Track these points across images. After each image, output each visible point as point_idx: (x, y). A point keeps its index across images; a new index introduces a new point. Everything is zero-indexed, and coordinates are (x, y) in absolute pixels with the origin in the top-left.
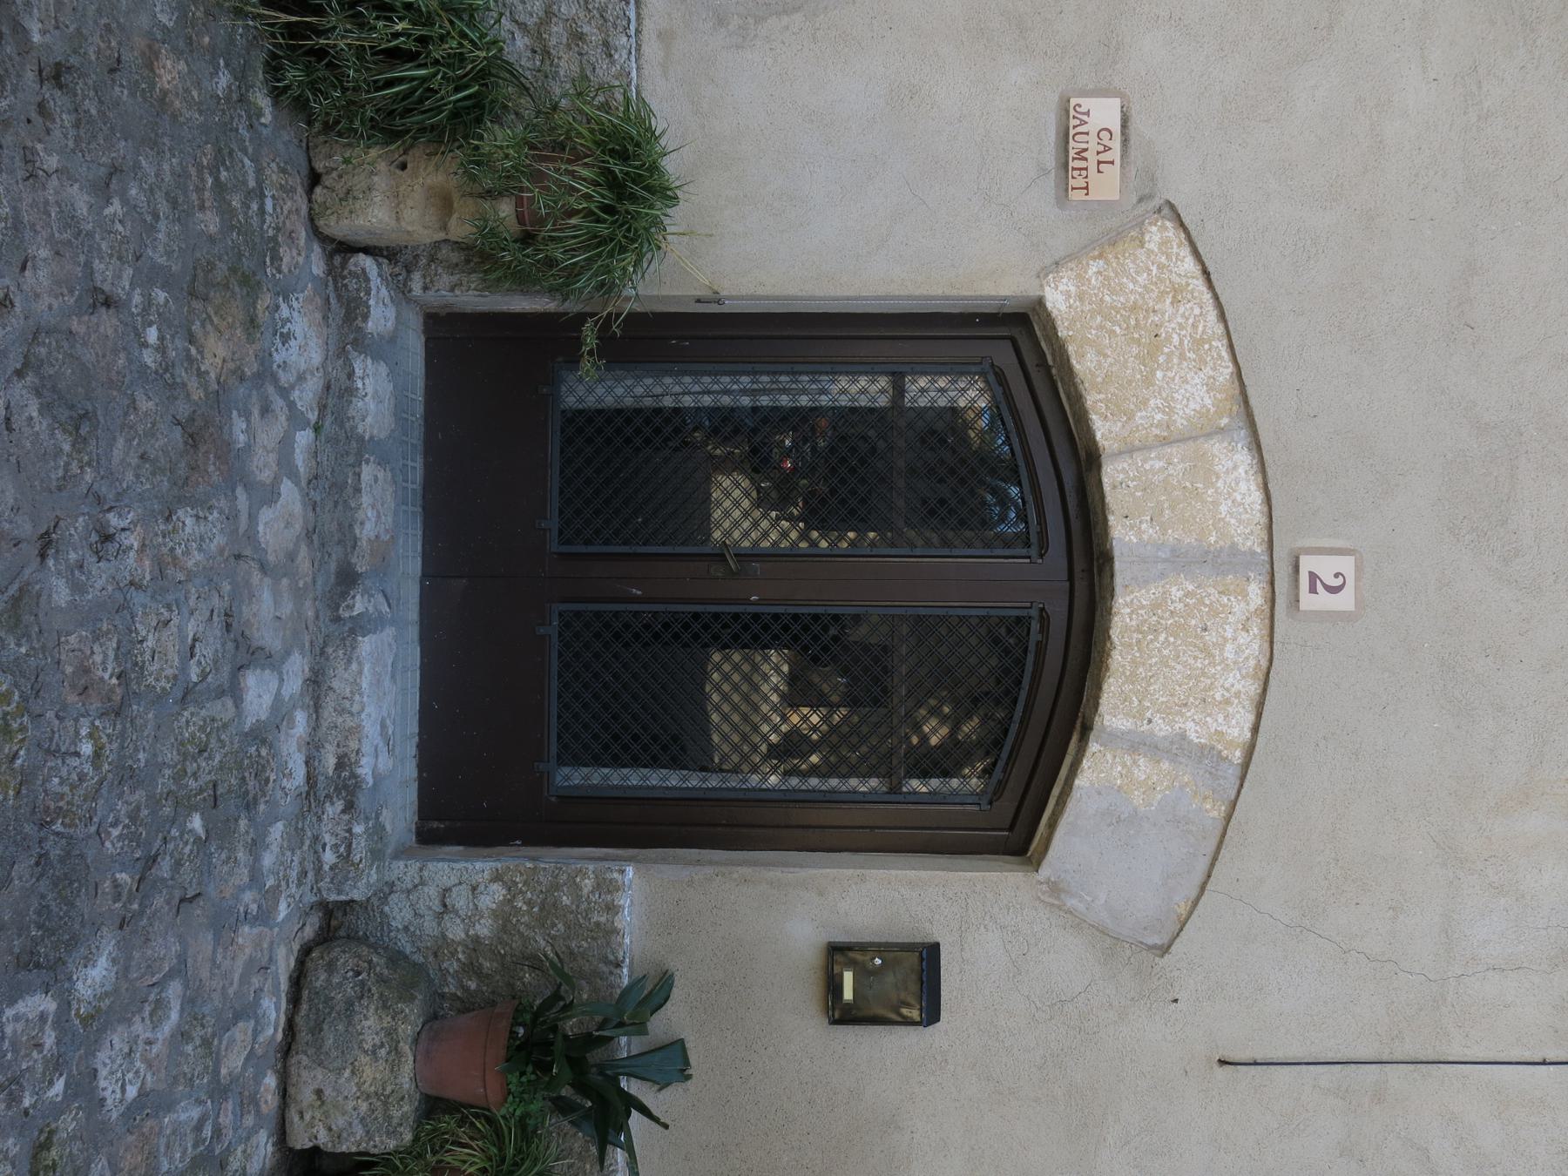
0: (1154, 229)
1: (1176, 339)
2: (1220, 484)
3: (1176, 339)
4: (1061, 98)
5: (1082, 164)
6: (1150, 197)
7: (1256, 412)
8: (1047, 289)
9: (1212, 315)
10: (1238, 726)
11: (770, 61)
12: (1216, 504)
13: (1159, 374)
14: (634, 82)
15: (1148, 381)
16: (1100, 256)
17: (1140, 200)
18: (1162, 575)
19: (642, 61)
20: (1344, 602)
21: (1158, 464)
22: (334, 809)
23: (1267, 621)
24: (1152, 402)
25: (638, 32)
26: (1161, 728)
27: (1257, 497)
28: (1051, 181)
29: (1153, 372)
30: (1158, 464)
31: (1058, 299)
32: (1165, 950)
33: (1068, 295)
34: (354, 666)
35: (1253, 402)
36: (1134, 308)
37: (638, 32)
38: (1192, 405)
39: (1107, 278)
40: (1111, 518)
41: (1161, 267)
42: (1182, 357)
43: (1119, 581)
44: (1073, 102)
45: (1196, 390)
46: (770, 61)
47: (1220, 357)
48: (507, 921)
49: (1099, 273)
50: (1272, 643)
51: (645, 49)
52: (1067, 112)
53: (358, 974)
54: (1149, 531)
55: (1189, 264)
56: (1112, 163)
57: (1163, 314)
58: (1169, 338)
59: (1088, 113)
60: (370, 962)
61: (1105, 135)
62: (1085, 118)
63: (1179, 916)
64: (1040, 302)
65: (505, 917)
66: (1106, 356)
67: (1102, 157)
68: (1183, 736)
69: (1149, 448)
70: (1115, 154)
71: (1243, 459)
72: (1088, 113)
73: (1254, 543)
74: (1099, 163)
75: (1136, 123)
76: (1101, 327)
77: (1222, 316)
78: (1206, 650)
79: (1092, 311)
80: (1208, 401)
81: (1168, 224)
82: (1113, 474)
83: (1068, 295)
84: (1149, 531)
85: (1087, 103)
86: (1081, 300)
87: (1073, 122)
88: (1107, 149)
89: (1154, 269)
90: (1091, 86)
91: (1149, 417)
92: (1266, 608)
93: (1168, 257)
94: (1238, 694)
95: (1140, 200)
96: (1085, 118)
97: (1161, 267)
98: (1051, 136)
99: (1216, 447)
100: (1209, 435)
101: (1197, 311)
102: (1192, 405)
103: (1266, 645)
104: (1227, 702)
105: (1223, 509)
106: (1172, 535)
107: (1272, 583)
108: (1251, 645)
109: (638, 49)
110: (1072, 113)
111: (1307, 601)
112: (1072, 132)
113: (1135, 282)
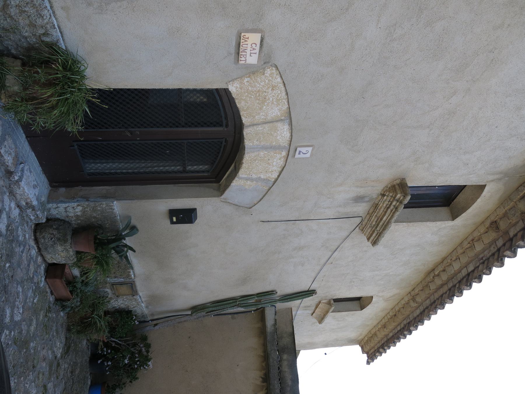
0: (269, 70)
1: (271, 99)
2: (279, 132)
3: (271, 99)
4: (238, 32)
5: (245, 53)
6: (268, 62)
7: (292, 118)
8: (229, 86)
9: (284, 93)
10: (275, 175)
11: (115, 19)
12: (276, 136)
13: (264, 107)
14: (56, 25)
15: (261, 109)
16: (249, 77)
17: (265, 63)
18: (259, 151)
19: (57, 16)
20: (308, 155)
21: (261, 129)
22: (29, 211)
23: (287, 152)
24: (261, 114)
25: (51, 7)
26: (254, 176)
27: (288, 135)
28: (233, 57)
29: (263, 107)
30: (261, 129)
31: (233, 88)
32: (251, 208)
33: (237, 87)
34: (21, 188)
35: (292, 116)
36: (259, 91)
37: (51, 7)
38: (274, 114)
39: (251, 83)
40: (245, 141)
41: (269, 81)
42: (273, 103)
43: (246, 152)
44: (243, 34)
45: (275, 111)
46: (115, 19)
47: (284, 104)
48: (84, 212)
49: (248, 82)
50: (286, 162)
51: (57, 12)
52: (240, 37)
53: (52, 239)
54: (256, 143)
55: (279, 79)
56: (256, 53)
57: (268, 93)
58: (269, 99)
59: (248, 38)
60: (53, 234)
61: (254, 45)
62: (247, 40)
63: (233, 318)
64: (228, 89)
65: (83, 211)
66: (248, 103)
67: (252, 52)
68: (260, 177)
69: (259, 124)
70: (257, 51)
71: (286, 127)
72: (248, 38)
73: (286, 144)
74: (251, 53)
75: (267, 40)
76: (247, 96)
77: (287, 94)
78: (269, 164)
79: (244, 92)
80: (279, 113)
81: (274, 68)
82: (246, 132)
83: (237, 87)
84: (256, 143)
85: (247, 35)
86: (241, 89)
87: (242, 41)
88: (254, 49)
89: (267, 81)
90: (250, 28)
91: (260, 117)
92: (286, 156)
93: (272, 78)
94: (275, 170)
95: (265, 63)
96: (247, 40)
97: (269, 81)
98: (234, 43)
99: (279, 125)
100: (277, 121)
101: (279, 92)
102: (274, 114)
103: (285, 163)
104: (272, 171)
105: (278, 138)
106: (262, 143)
107: (289, 152)
108: (281, 163)
109: (54, 12)
110: (242, 38)
111: (297, 156)
112: (241, 44)
113: (259, 84)
